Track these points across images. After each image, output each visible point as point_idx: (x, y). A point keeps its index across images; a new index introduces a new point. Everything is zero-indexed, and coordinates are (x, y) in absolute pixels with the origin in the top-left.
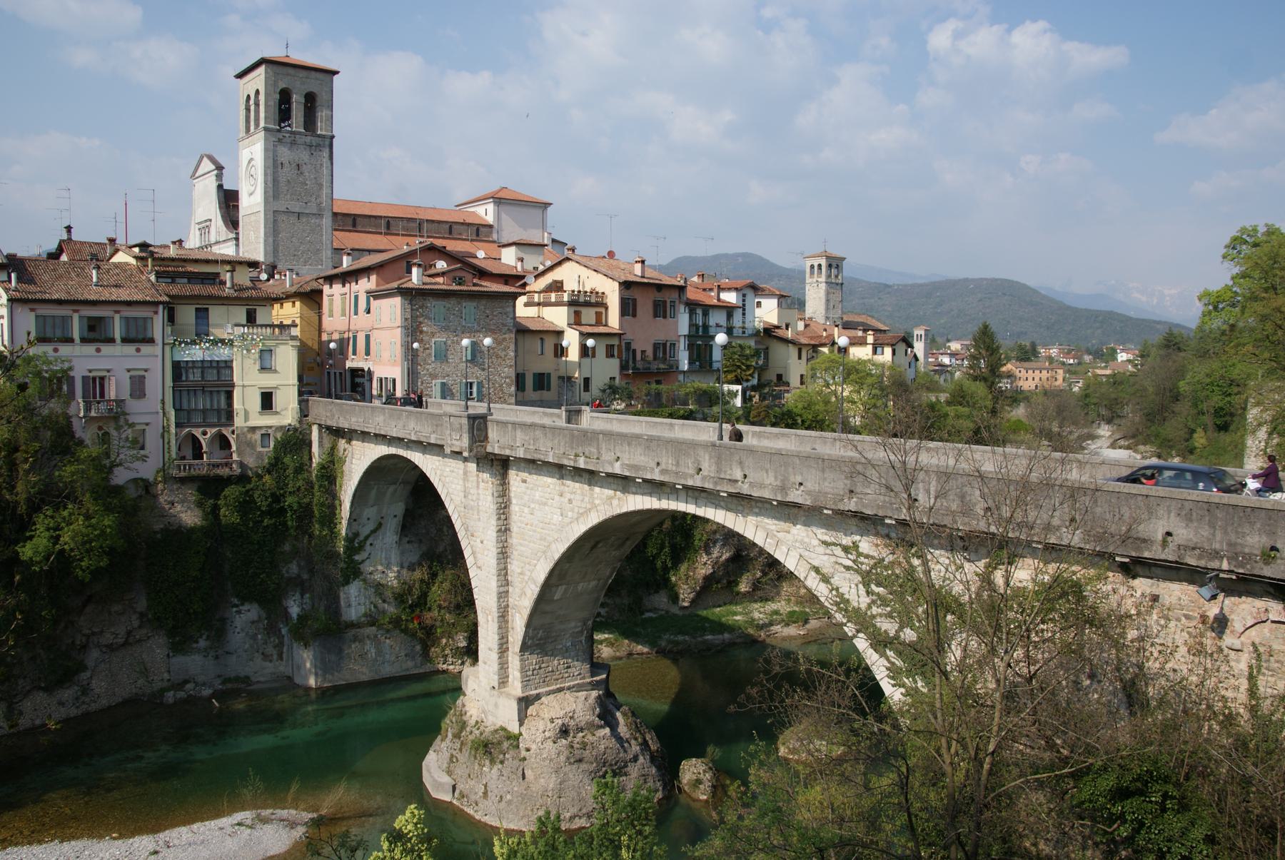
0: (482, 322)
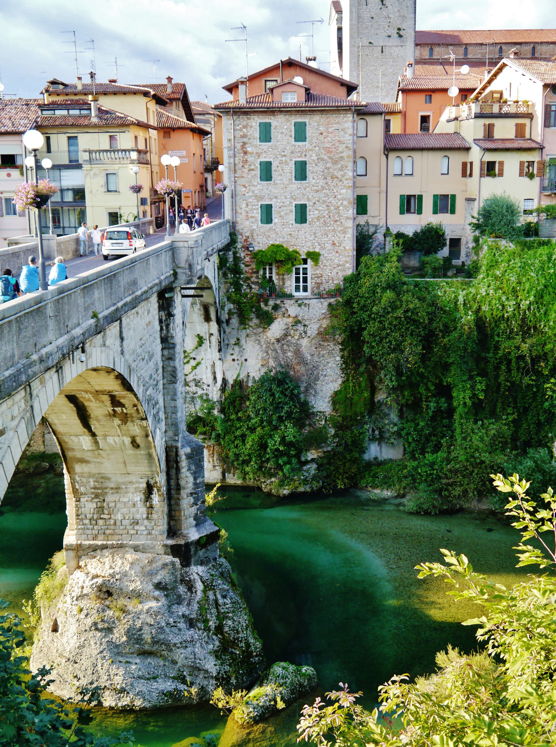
0: (314, 141)
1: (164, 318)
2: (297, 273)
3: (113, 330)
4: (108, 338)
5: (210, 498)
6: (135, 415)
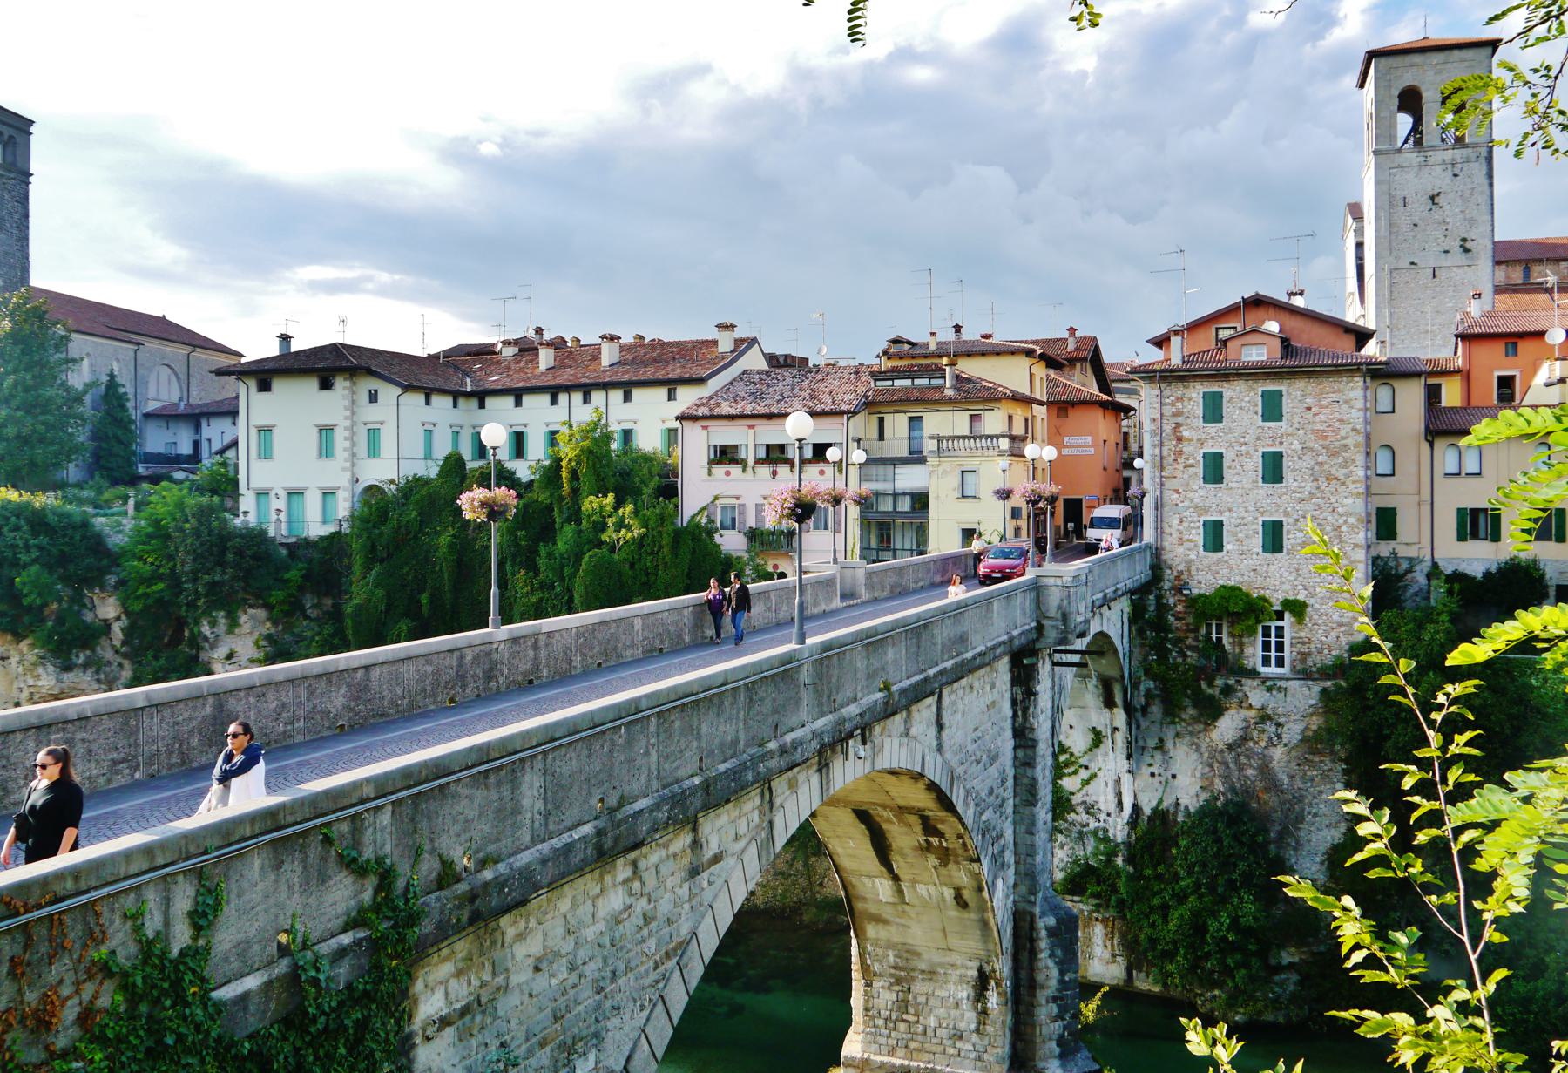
0: (1297, 419)
1: (1020, 697)
2: (1266, 633)
3: (926, 708)
4: (914, 723)
5: (1089, 1010)
6: (960, 851)
